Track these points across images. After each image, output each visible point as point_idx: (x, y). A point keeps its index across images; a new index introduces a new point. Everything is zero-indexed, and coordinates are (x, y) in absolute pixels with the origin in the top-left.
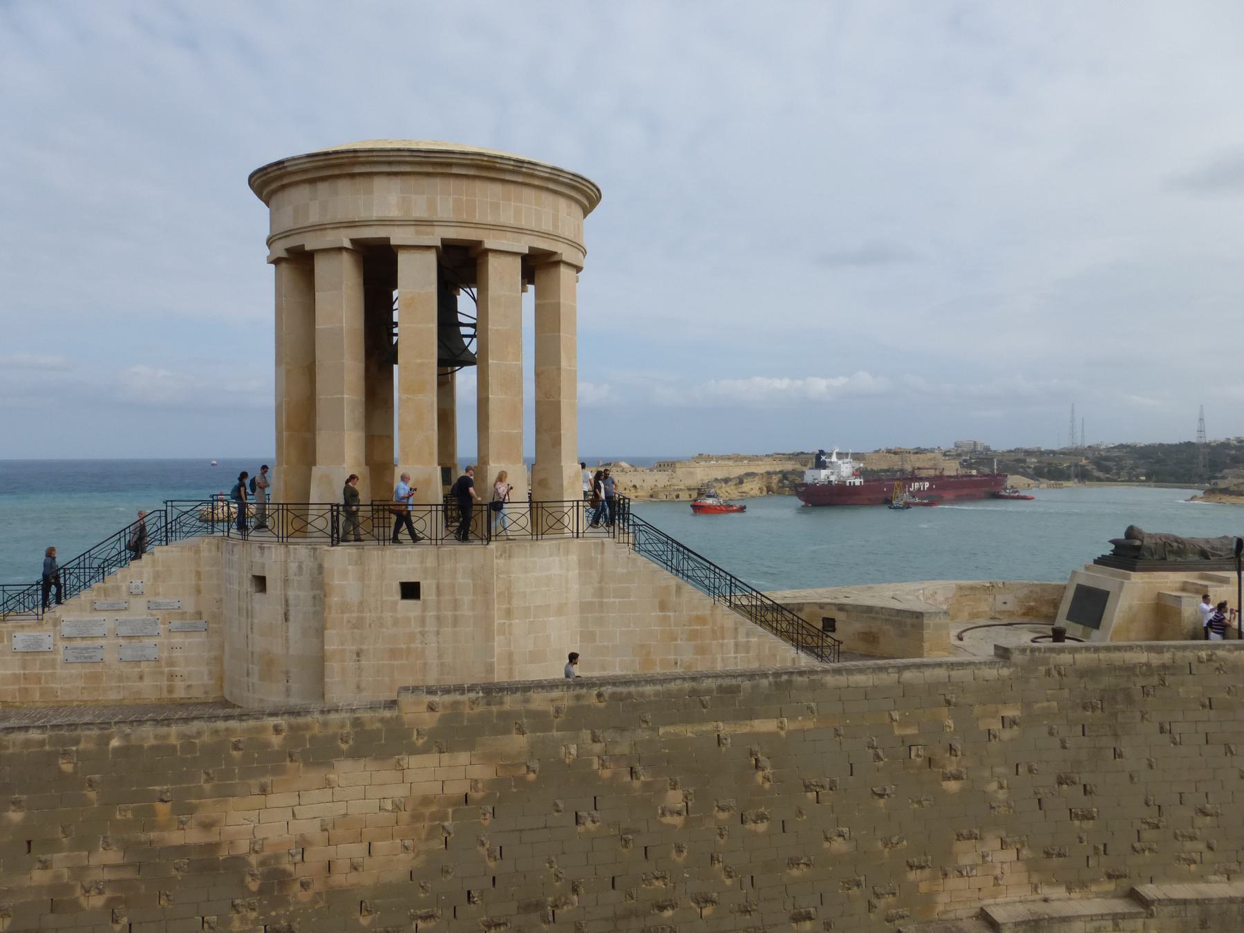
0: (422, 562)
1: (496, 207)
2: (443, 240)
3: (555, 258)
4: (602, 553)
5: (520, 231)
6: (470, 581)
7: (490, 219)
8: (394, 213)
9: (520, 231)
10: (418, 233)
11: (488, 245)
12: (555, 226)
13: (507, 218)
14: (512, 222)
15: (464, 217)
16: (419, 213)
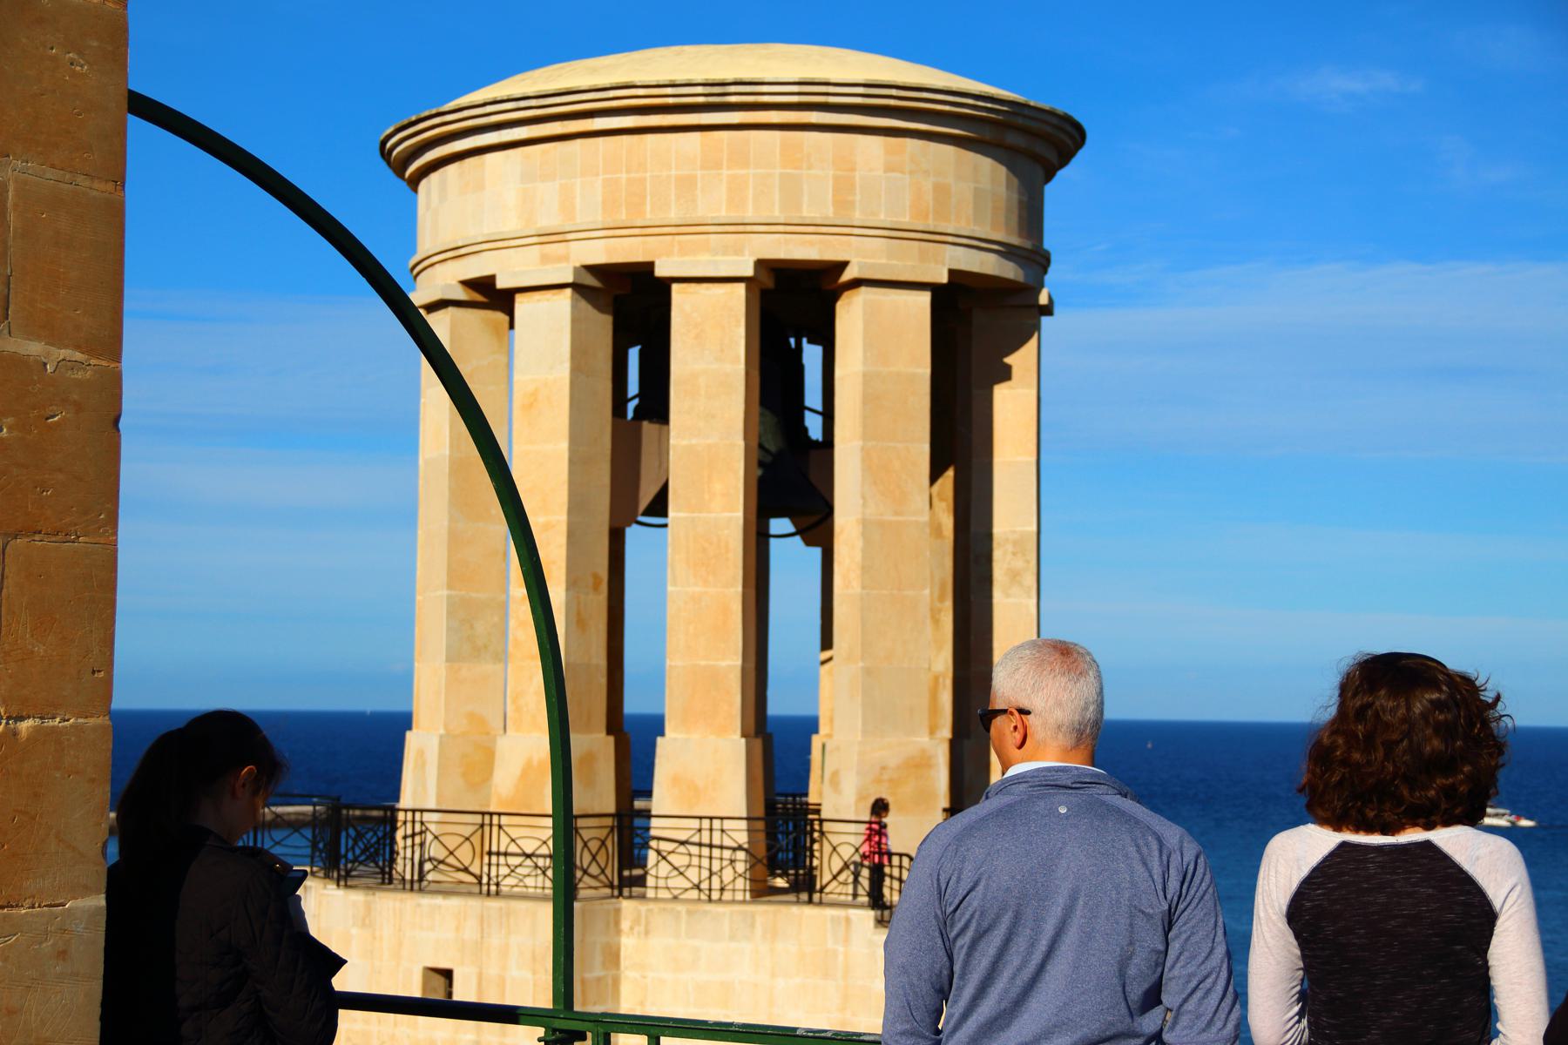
0: (457, 929)
1: (687, 184)
2: (591, 269)
3: (847, 275)
4: (846, 941)
5: (739, 227)
6: (529, 975)
7: (673, 216)
8: (511, 225)
9: (739, 227)
10: (545, 259)
11: (660, 272)
12: (842, 203)
13: (713, 205)
14: (723, 214)
15: (622, 217)
16: (549, 220)
